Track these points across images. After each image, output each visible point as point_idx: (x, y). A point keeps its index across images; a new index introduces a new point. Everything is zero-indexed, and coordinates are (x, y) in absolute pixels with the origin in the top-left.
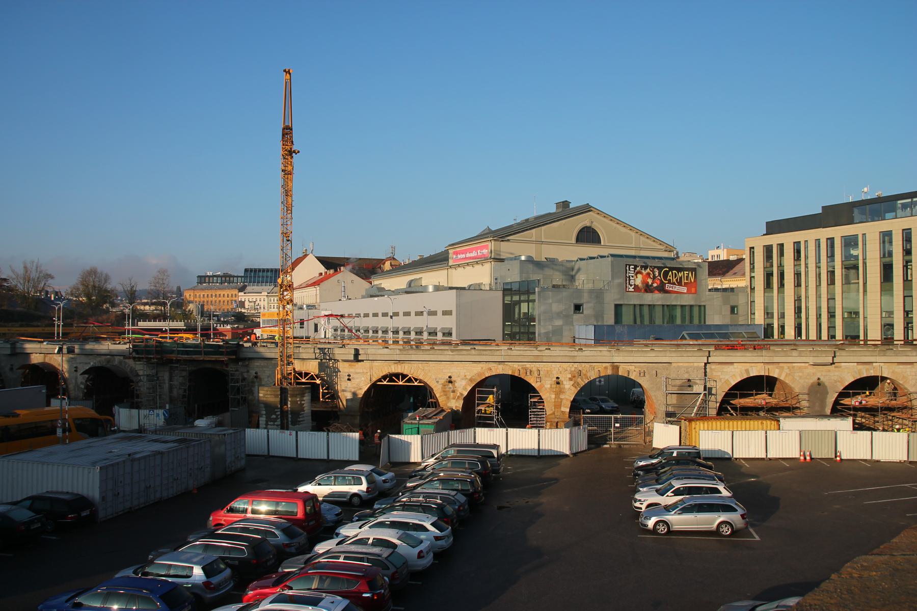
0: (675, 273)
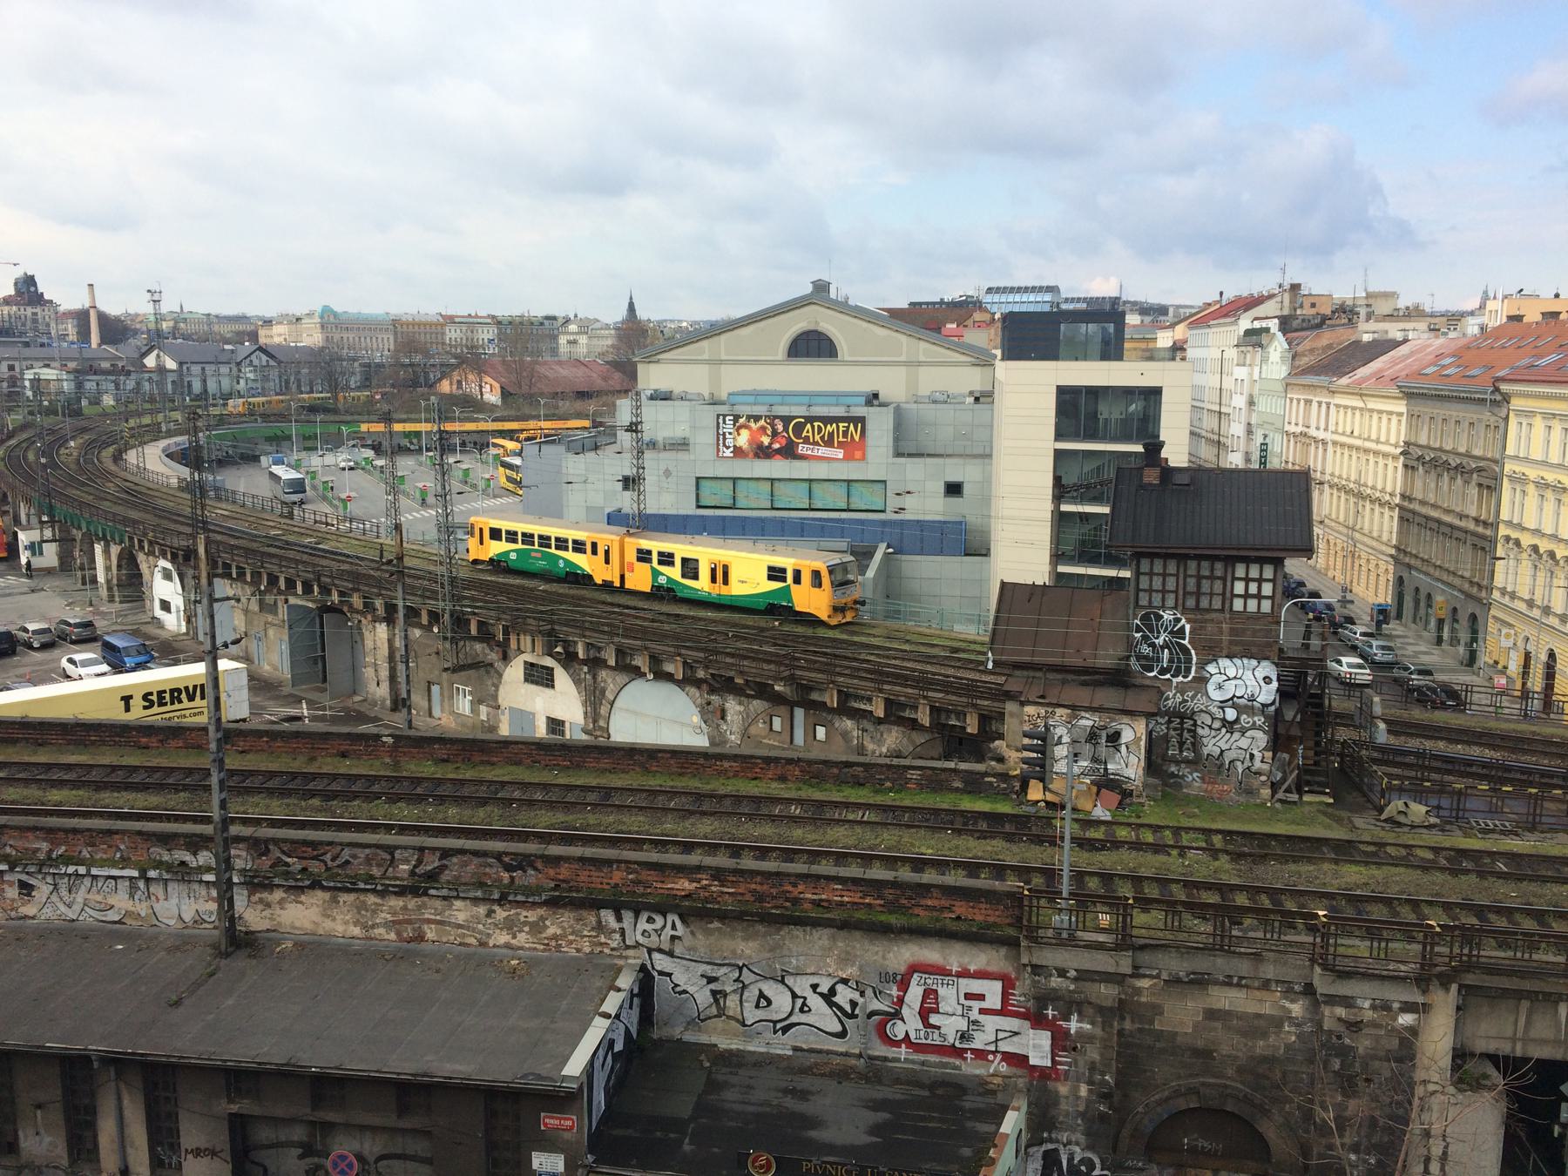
0: (819, 426)
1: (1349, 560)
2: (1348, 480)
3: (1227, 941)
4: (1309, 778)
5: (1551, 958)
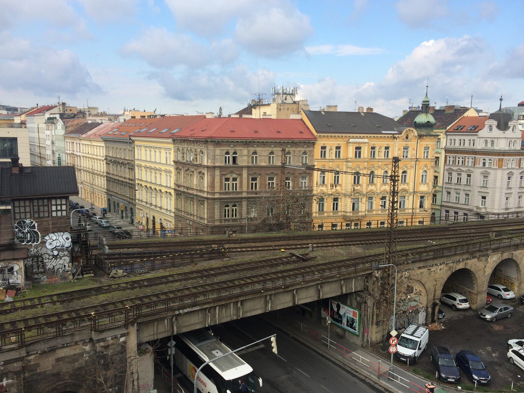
1: (92, 195)
2: (89, 168)
3: (61, 332)
4: (85, 269)
5: (161, 307)
